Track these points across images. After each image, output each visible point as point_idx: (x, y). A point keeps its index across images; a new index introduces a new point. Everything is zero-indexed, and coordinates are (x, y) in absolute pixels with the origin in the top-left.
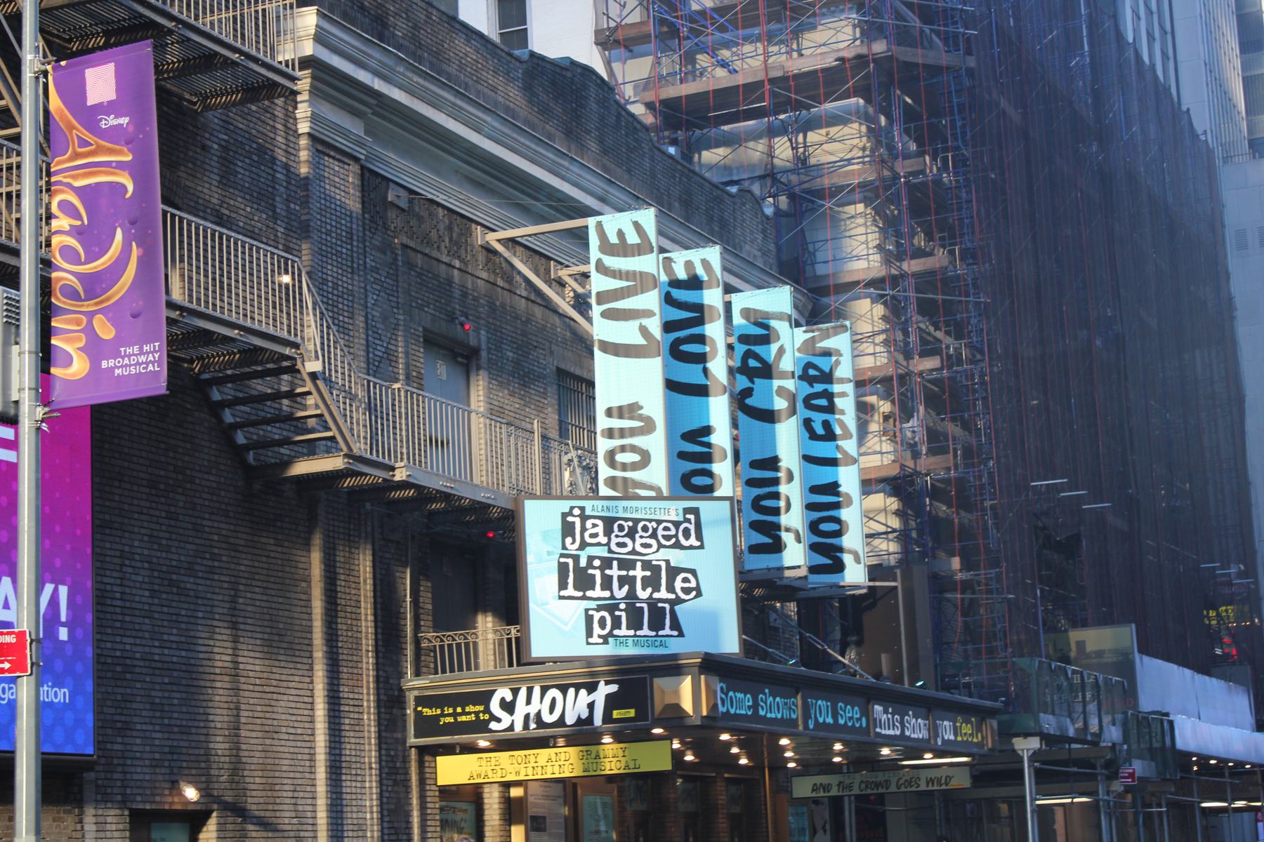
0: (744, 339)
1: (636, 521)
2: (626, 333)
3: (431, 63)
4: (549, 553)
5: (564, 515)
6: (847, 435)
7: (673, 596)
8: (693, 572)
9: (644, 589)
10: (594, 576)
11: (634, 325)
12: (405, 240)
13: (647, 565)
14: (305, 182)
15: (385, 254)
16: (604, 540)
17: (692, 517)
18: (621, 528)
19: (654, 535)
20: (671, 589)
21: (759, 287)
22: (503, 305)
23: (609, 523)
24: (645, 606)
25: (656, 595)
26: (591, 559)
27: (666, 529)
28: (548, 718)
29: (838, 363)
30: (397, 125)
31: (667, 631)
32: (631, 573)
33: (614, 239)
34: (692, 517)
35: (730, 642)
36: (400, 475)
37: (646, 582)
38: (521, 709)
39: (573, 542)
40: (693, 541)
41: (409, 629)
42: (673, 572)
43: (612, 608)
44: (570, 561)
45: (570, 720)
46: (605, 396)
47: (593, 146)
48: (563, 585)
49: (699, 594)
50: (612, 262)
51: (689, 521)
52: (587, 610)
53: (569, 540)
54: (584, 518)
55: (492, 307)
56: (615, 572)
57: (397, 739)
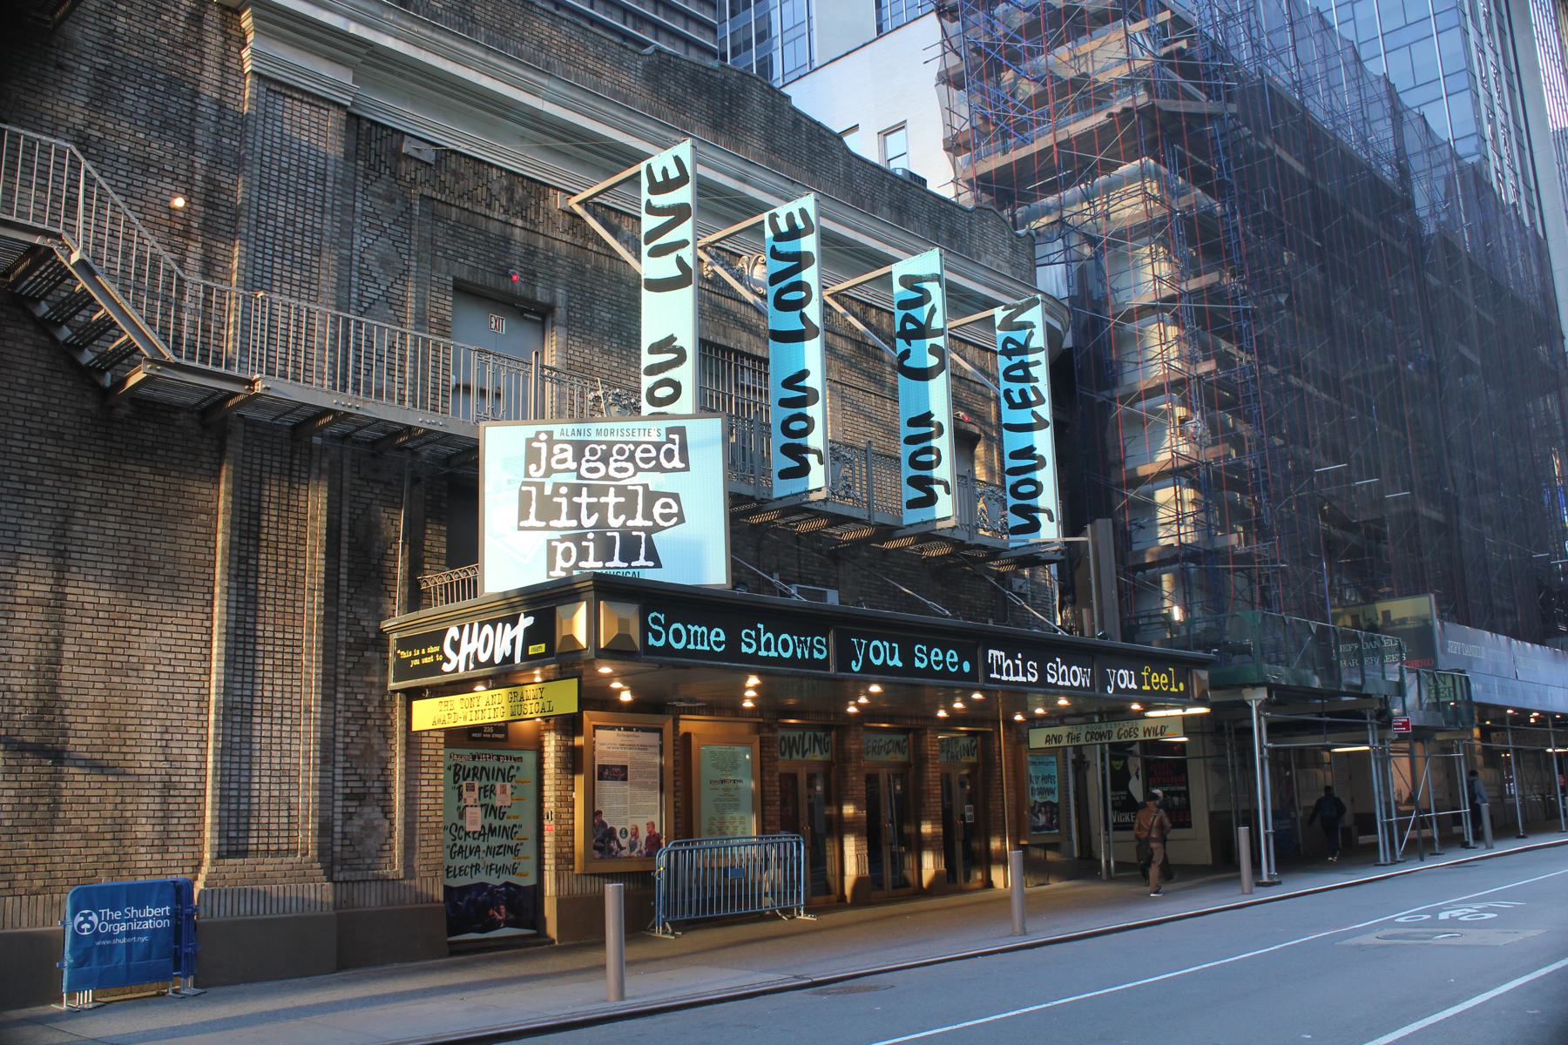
0: (903, 305)
1: (611, 444)
2: (665, 267)
3: (577, 75)
4: (509, 481)
5: (529, 441)
6: (1041, 401)
7: (650, 524)
8: (676, 497)
9: (616, 517)
10: (560, 504)
11: (672, 257)
12: (427, 192)
13: (621, 491)
14: (242, 120)
15: (392, 201)
16: (574, 466)
17: (676, 437)
18: (594, 452)
19: (631, 458)
20: (648, 515)
21: (914, 254)
22: (598, 269)
23: (579, 448)
24: (617, 535)
25: (630, 523)
26: (557, 486)
27: (646, 451)
28: (483, 658)
29: (1031, 334)
30: (412, 80)
31: (642, 562)
32: (603, 500)
33: (659, 178)
34: (676, 437)
35: (714, 571)
36: (259, 388)
37: (619, 510)
38: (465, 648)
39: (539, 468)
40: (677, 463)
41: (400, 570)
42: (651, 497)
43: (578, 539)
44: (533, 490)
45: (498, 660)
46: (650, 333)
47: (757, 144)
48: (524, 515)
49: (681, 520)
50: (660, 200)
51: (673, 441)
52: (549, 542)
53: (533, 467)
54: (551, 442)
55: (579, 271)
56: (584, 500)
57: (372, 684)
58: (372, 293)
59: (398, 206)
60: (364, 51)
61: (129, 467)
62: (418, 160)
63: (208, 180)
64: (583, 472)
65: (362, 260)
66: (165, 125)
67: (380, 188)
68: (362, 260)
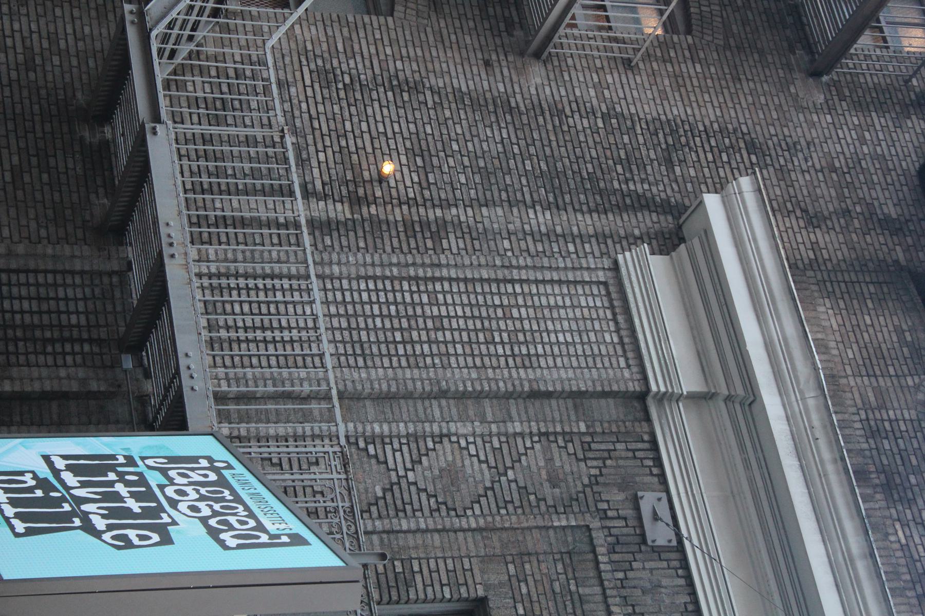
8: (166, 540)
12: (599, 537)
30: (751, 481)
31: (20, 526)
56: (120, 488)
58: (397, 459)
59: (547, 490)
60: (740, 391)
61: (13, 141)
62: (640, 518)
63: (443, 224)
64: (170, 491)
65: (440, 438)
66: (485, 173)
67: (562, 461)
68: (440, 438)
